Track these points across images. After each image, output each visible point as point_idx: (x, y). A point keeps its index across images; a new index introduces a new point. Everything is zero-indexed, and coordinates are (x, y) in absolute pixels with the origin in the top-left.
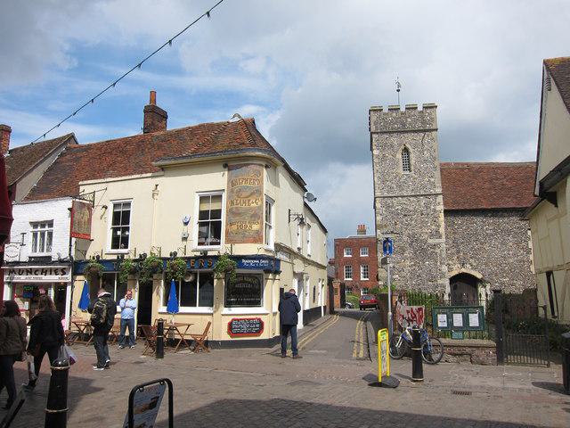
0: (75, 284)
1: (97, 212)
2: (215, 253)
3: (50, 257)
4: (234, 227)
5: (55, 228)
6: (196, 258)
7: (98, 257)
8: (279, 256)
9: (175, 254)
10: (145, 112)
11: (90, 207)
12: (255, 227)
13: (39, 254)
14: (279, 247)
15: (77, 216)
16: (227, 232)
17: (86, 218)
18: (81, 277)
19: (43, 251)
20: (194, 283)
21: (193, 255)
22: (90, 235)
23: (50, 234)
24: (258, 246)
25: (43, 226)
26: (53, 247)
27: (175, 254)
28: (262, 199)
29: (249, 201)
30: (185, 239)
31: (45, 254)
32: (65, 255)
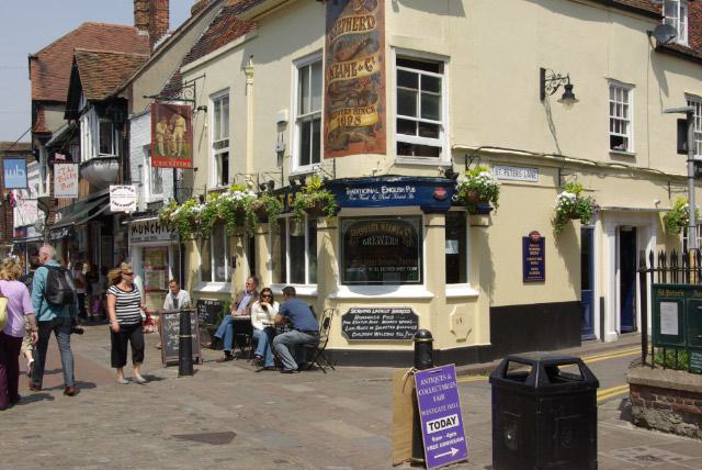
1: (198, 120)
4: (334, 124)
8: (490, 175)
9: (272, 184)
11: (186, 114)
12: (368, 119)
14: (468, 156)
16: (326, 129)
17: (180, 131)
20: (302, 238)
22: (192, 162)
24: (375, 157)
27: (272, 184)
28: (382, 59)
29: (354, 64)
30: (281, 154)
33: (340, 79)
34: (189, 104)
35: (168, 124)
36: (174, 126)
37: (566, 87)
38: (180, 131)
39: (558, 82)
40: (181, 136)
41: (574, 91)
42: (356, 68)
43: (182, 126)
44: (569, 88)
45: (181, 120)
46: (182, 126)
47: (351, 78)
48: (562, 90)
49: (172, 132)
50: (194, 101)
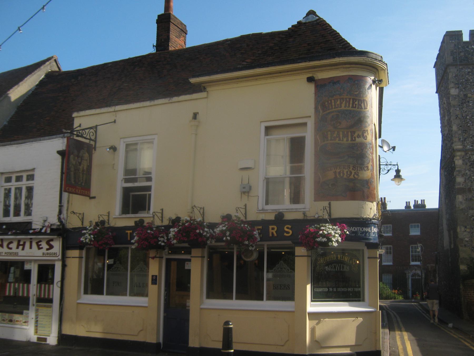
0: (69, 262)
2: (299, 216)
3: (30, 223)
5: (36, 184)
6: (265, 224)
7: (103, 222)
10: (158, 22)
13: (12, 219)
15: (73, 160)
18: (75, 253)
19: (17, 213)
21: (262, 217)
23: (30, 190)
25: (19, 179)
26: (35, 209)
31: (22, 218)
32: (54, 220)
33: (337, 141)
34: (92, 143)
35: (78, 157)
36: (82, 160)
37: (396, 171)
38: (85, 164)
39: (390, 167)
40: (85, 168)
41: (401, 174)
42: (356, 134)
43: (87, 160)
44: (398, 171)
45: (86, 155)
46: (87, 160)
47: (349, 142)
48: (393, 173)
49: (80, 164)
50: (95, 141)
